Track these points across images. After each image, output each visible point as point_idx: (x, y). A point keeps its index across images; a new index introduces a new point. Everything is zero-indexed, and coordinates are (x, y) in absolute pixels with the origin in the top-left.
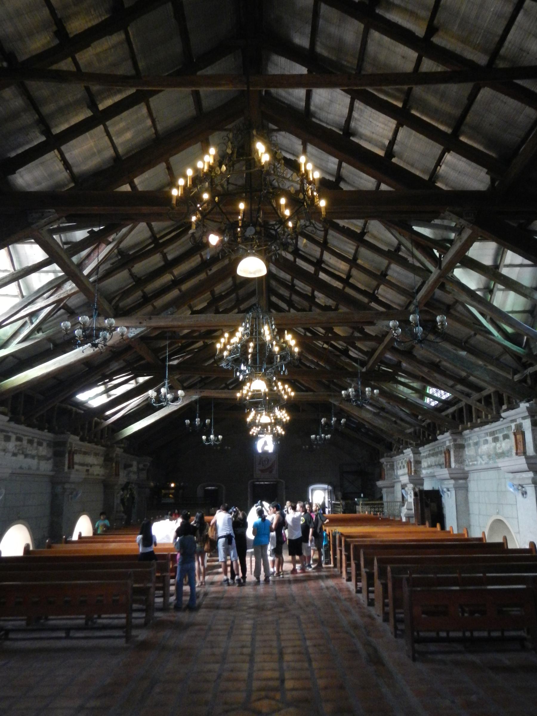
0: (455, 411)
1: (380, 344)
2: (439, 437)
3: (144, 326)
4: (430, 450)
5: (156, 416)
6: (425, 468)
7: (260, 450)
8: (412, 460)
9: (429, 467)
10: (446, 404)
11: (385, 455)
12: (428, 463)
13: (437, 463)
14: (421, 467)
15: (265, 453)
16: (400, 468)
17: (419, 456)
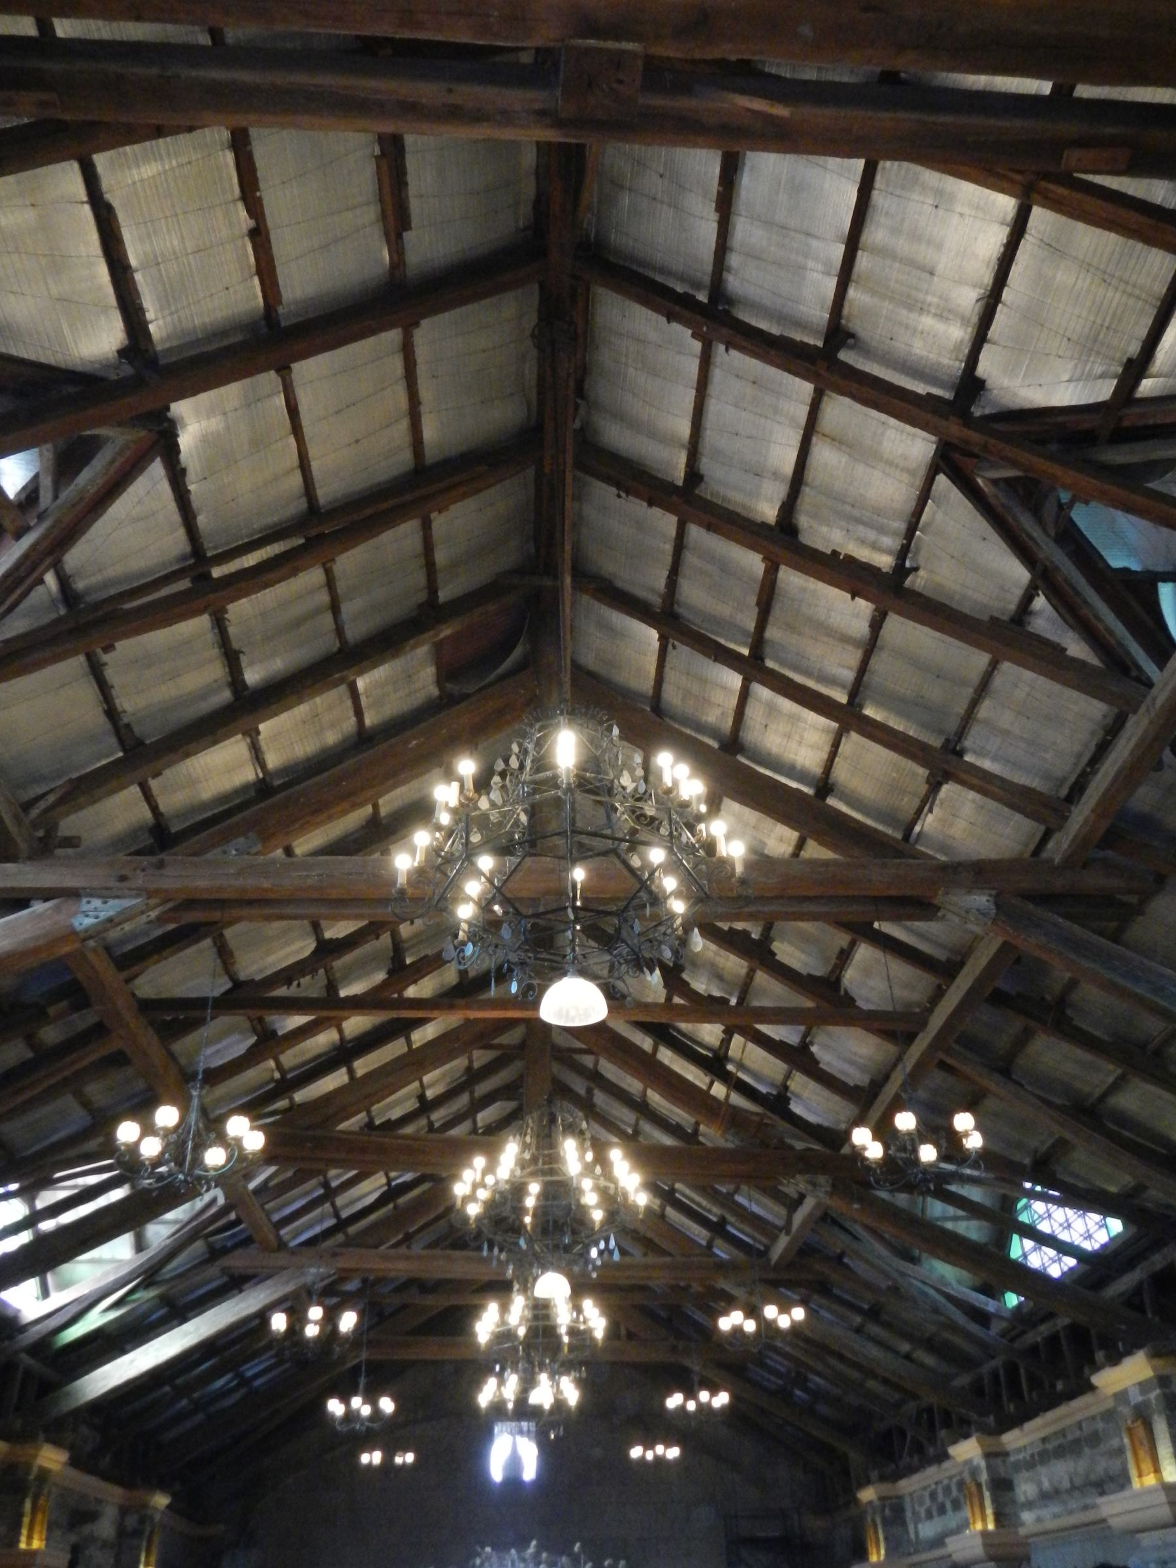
0: (1138, 1290)
1: (910, 1038)
2: (1096, 1380)
3: (139, 892)
4: (1044, 1440)
5: (186, 1334)
6: (1029, 1505)
7: (497, 1472)
8: (984, 1477)
9: (1046, 1497)
10: (1097, 1267)
11: (874, 1474)
12: (1039, 1484)
13: (1078, 1481)
14: (1014, 1501)
15: (513, 1481)
16: (929, 1516)
17: (1004, 1462)
